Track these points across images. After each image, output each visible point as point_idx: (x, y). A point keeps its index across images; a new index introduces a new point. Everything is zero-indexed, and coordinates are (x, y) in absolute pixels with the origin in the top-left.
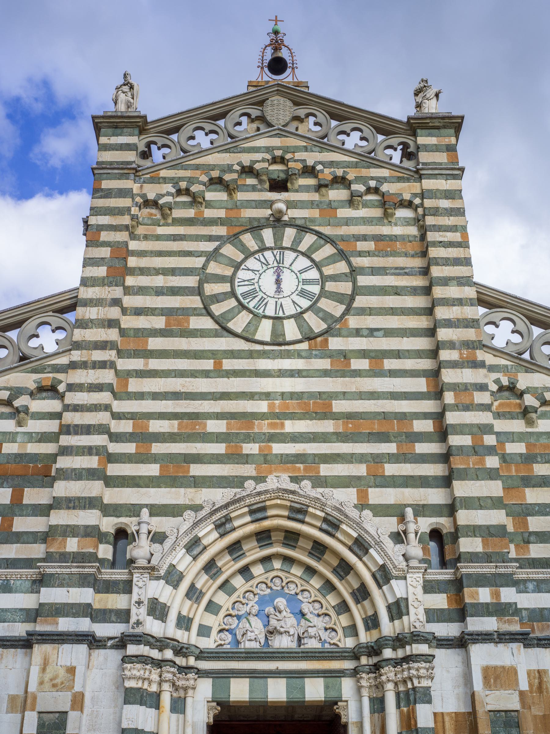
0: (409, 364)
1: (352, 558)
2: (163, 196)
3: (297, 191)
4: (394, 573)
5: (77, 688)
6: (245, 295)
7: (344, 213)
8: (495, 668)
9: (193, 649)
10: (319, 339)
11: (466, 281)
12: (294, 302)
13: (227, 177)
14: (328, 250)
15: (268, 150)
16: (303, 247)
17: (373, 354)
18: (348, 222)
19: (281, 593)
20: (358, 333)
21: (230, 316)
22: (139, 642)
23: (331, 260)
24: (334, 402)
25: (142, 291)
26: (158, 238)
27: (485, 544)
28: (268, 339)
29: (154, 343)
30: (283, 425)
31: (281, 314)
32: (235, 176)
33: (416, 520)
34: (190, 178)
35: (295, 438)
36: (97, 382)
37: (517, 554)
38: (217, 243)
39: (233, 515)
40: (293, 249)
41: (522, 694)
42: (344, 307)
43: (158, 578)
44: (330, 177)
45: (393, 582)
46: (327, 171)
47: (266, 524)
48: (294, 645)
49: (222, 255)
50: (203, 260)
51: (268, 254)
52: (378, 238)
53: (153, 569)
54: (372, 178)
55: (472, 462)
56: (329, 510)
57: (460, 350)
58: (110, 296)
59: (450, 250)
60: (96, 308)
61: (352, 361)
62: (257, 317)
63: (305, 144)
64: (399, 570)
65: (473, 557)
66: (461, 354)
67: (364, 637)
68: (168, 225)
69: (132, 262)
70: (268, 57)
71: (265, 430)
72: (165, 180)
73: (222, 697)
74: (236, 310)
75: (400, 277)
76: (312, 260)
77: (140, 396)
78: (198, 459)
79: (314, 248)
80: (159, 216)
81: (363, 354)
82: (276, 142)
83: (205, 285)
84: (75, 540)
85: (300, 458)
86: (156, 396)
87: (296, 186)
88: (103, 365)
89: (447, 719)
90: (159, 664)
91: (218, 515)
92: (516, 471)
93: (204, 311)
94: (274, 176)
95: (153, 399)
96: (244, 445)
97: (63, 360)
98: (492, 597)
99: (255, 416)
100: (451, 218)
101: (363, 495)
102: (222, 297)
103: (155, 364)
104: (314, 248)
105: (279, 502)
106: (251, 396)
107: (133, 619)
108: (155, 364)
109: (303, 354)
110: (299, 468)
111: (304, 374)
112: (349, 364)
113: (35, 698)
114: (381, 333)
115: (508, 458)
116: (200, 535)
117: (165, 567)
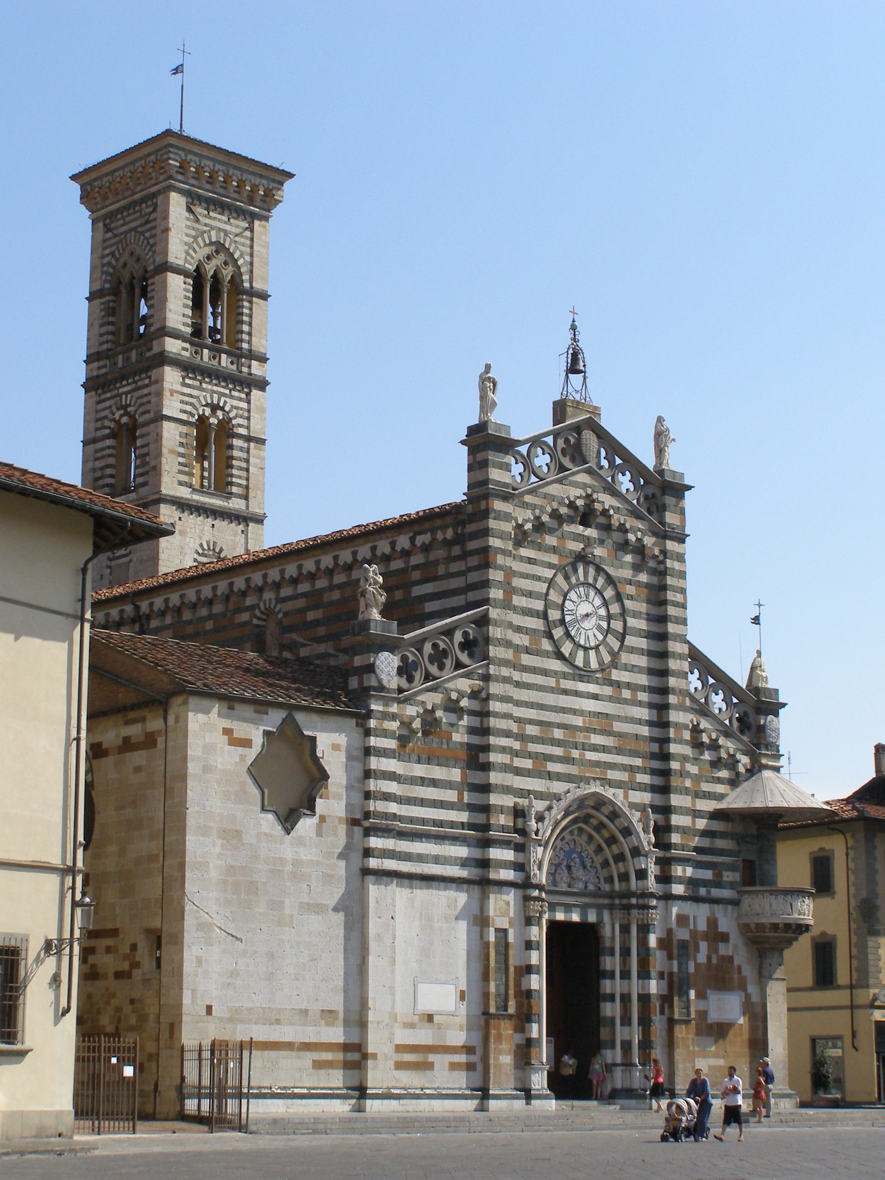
1: (621, 839)
4: (643, 853)
11: (683, 639)
12: (595, 636)
15: (585, 486)
20: (626, 668)
26: (522, 559)
28: (581, 665)
30: (590, 737)
31: (588, 645)
35: (595, 748)
43: (540, 845)
44: (617, 524)
45: (641, 858)
46: (616, 516)
47: (585, 811)
53: (541, 840)
56: (616, 808)
65: (676, 846)
66: (679, 699)
73: (552, 918)
81: (628, 685)
85: (598, 764)
88: (506, 680)
99: (575, 728)
101: (626, 796)
103: (527, 678)
106: (574, 712)
108: (527, 678)
109: (599, 680)
110: (597, 772)
112: (621, 694)
113: (493, 920)
114: (635, 669)
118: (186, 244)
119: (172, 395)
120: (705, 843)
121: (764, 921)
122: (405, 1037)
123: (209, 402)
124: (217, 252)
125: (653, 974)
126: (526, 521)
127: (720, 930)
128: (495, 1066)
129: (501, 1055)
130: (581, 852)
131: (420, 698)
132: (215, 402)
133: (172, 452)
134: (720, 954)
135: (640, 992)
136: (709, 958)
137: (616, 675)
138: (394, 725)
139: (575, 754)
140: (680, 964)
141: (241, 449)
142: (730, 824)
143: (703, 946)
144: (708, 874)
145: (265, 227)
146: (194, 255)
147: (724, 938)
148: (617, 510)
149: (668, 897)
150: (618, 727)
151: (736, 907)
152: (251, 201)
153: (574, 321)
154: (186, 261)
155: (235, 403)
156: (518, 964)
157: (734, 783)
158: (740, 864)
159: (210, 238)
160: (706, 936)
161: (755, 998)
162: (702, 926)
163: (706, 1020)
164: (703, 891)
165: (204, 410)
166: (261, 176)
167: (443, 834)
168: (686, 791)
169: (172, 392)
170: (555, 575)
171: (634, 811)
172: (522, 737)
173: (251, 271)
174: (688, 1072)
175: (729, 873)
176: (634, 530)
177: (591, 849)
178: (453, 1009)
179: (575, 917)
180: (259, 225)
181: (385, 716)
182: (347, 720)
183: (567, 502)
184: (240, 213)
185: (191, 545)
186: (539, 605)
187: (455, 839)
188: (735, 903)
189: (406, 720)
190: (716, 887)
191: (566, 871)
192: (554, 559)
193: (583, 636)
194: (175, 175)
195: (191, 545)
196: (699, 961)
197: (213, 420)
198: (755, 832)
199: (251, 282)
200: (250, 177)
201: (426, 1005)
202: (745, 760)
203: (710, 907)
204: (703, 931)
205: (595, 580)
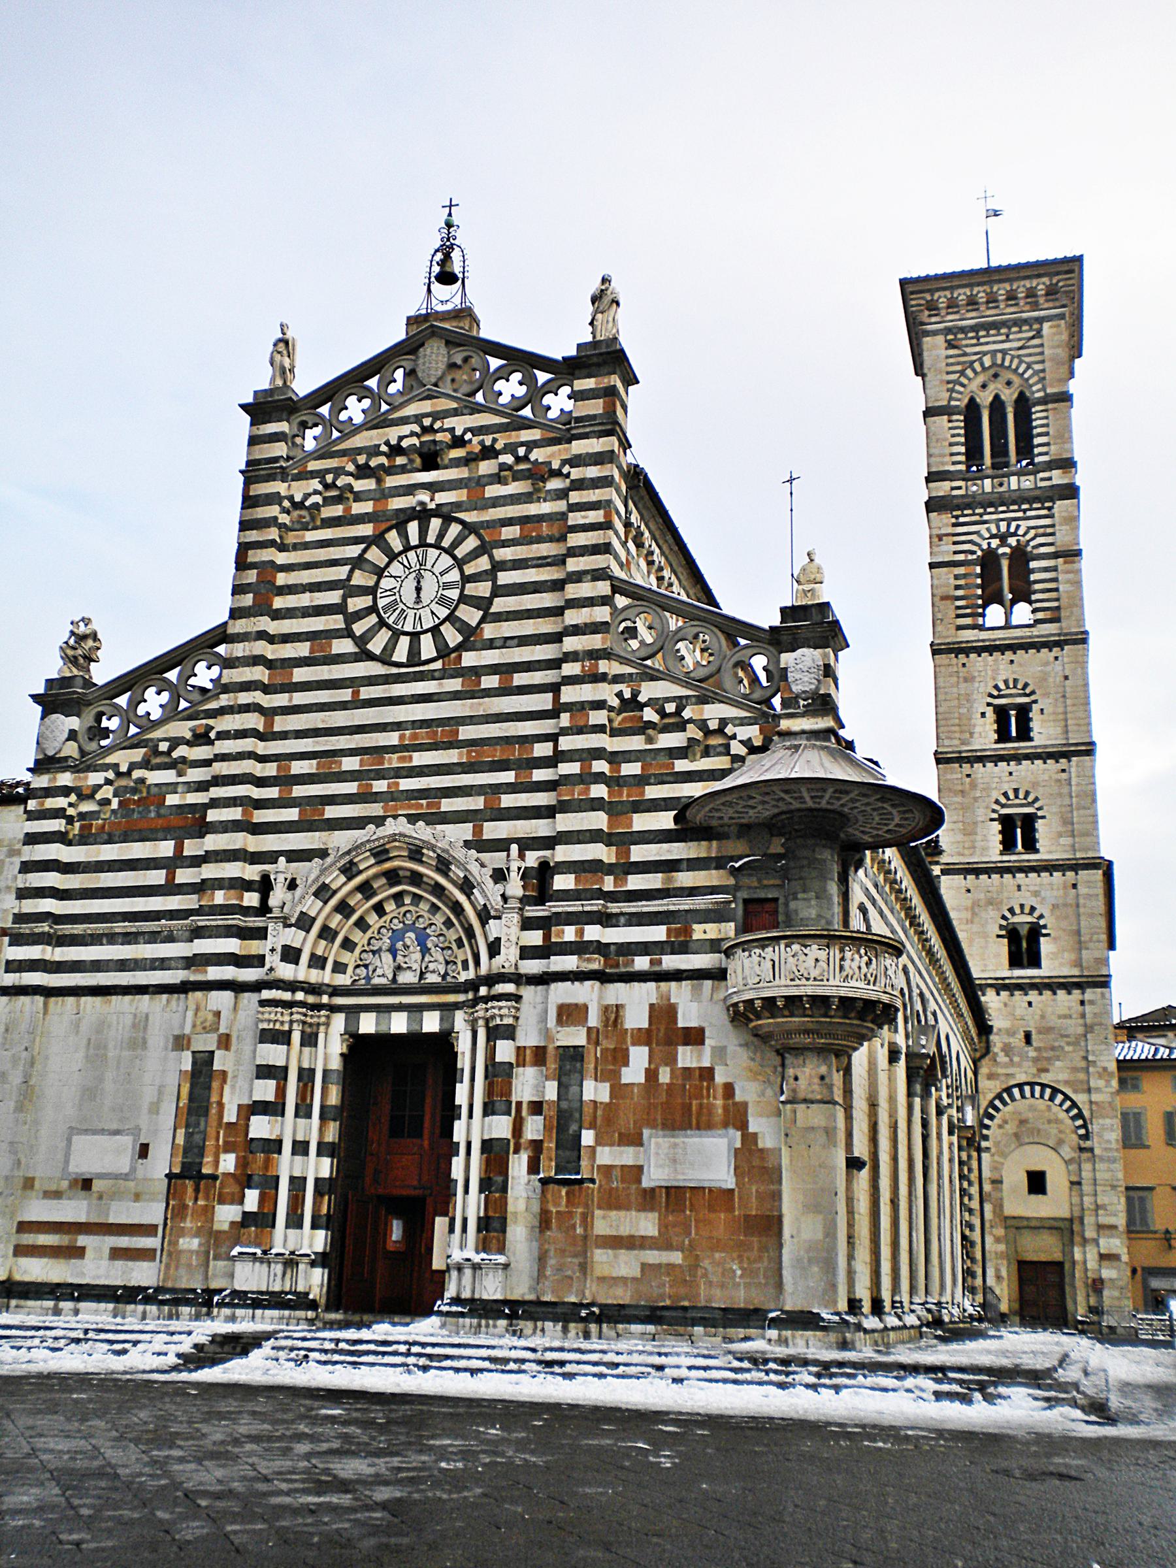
0: (538, 678)
1: (462, 898)
2: (310, 495)
3: (446, 467)
4: (493, 913)
5: (222, 1030)
6: (385, 608)
7: (492, 491)
8: (569, 1005)
9: (324, 988)
10: (453, 655)
12: (432, 613)
13: (373, 463)
14: (472, 543)
15: (418, 419)
16: (446, 543)
17: (504, 669)
18: (496, 502)
19: (412, 928)
20: (491, 644)
21: (370, 634)
22: (271, 988)
23: (474, 555)
24: (461, 728)
25: (289, 613)
26: (306, 546)
27: (577, 880)
29: (300, 674)
30: (411, 758)
31: (419, 629)
32: (383, 460)
33: (522, 856)
34: (336, 468)
36: (241, 728)
37: (615, 886)
38: (363, 546)
39: (356, 860)
40: (436, 546)
41: (589, 1029)
42: (481, 613)
43: (290, 926)
44: (477, 449)
45: (491, 921)
46: (475, 440)
47: (388, 865)
48: (416, 980)
49: (366, 560)
50: (348, 568)
51: (411, 555)
52: (523, 521)
53: (285, 918)
54: (522, 444)
55: (577, 793)
56: (439, 851)
57: (583, 661)
58: (256, 629)
59: (590, 533)
60: (241, 645)
61: (483, 678)
62: (397, 634)
63: (455, 405)
64: (496, 910)
65: (565, 895)
66: (583, 666)
67: (470, 974)
68: (315, 528)
69: (281, 579)
70: (436, 269)
71: (395, 765)
72: (313, 475)
73: (352, 1029)
74: (377, 628)
75: (541, 569)
76: (454, 557)
77: (284, 735)
78: (332, 800)
79: (457, 543)
80: (308, 519)
81: (494, 669)
82: (426, 406)
83: (349, 600)
84: (222, 892)
86: (300, 734)
87: (446, 461)
89: (528, 1052)
90: (289, 1005)
91: (343, 862)
92: (628, 795)
93: (345, 633)
94: (425, 450)
95: (296, 738)
96: (374, 782)
97: (213, 705)
98: (576, 935)
100: (597, 491)
101: (478, 830)
102: (364, 613)
103: (300, 698)
104: (457, 543)
105: (397, 844)
107: (267, 966)
108: (300, 698)
111: (435, 698)
112: (479, 683)
114: (516, 641)
115: (621, 781)
116: (327, 882)
117: (296, 915)
118: (948, 382)
119: (940, 540)
120: (653, 881)
121: (735, 999)
122: (39, 1210)
123: (994, 531)
124: (996, 376)
125: (500, 1106)
126: (307, 496)
127: (680, 1025)
128: (170, 1254)
129: (183, 1236)
130: (425, 929)
131: (110, 759)
132: (1003, 528)
133: (944, 598)
134: (680, 1065)
135: (486, 1137)
136: (651, 1074)
137: (469, 659)
138: (60, 802)
139: (380, 786)
140: (562, 1088)
141: (1046, 570)
142: (714, 843)
143: (639, 1057)
144: (658, 933)
145: (1059, 326)
146: (962, 389)
147: (695, 1037)
148: (475, 431)
149: (544, 979)
150: (467, 733)
151: (724, 983)
152: (1035, 306)
153: (450, 215)
154: (951, 399)
155: (1032, 523)
156: (246, 1101)
157: (723, 774)
158: (737, 907)
159: (982, 364)
160: (644, 1037)
161: (767, 1142)
162: (636, 1018)
163: (639, 1181)
164: (642, 963)
165: (989, 544)
166: (1039, 276)
167: (134, 930)
168: (596, 805)
169: (940, 538)
170: (365, 551)
171: (473, 852)
172: (286, 780)
174: (569, 1273)
175: (708, 926)
176: (511, 448)
177: (439, 919)
178: (126, 1170)
179: (399, 1024)
180: (1051, 327)
181: (48, 792)
182: (13, 808)
183: (384, 448)
184: (1019, 323)
185: (981, 690)
186: (334, 597)
187: (153, 937)
188: (719, 975)
189: (86, 792)
190: (672, 953)
191: (387, 958)
192: (367, 530)
193: (410, 620)
194: (927, 320)
195: (981, 690)
196: (624, 1081)
198: (782, 851)
199: (1044, 389)
200: (1022, 283)
201: (82, 1165)
202: (752, 732)
203: (658, 987)
204: (640, 1029)
205: (441, 536)
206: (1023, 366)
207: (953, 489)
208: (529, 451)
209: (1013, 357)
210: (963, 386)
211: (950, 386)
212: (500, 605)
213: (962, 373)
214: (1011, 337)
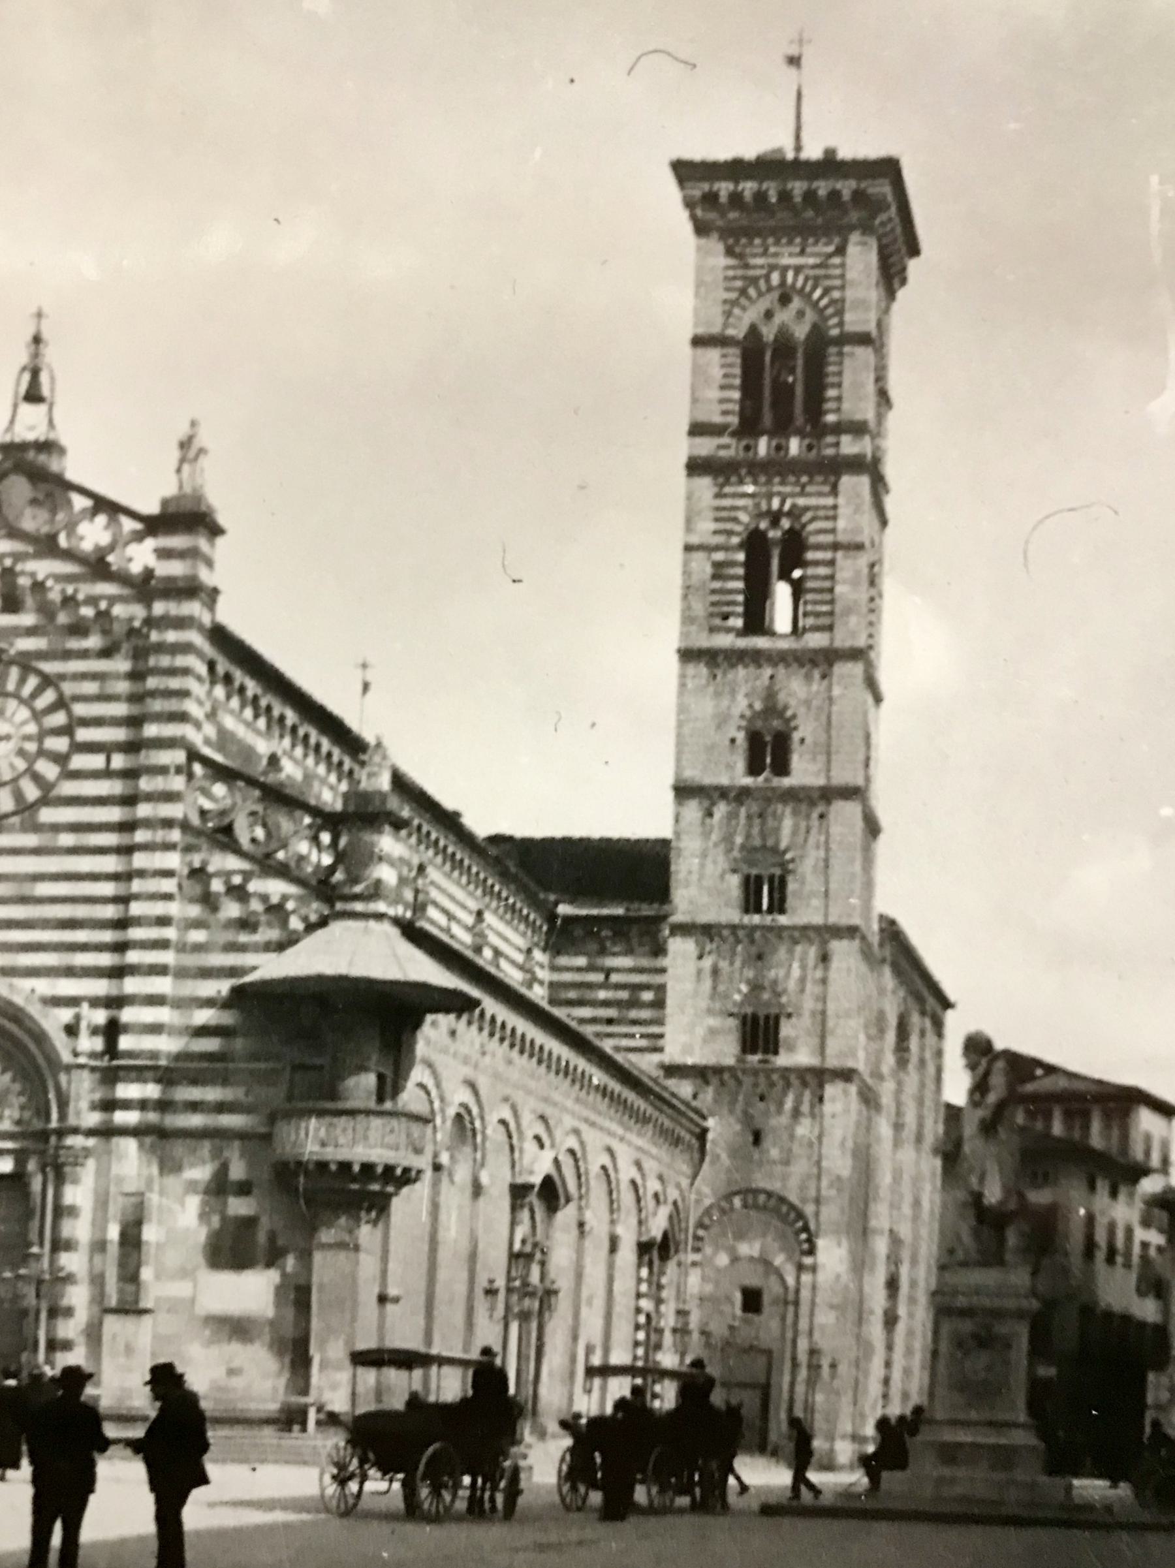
14: (49, 697)
40: (16, 695)
46: (58, 587)
137: (47, 815)
148: (59, 578)
173: (840, 313)
176: (92, 601)
197: (775, 534)
199: (841, 324)
206: (817, 293)
207: (720, 447)
208: (111, 605)
209: (807, 279)
210: (744, 309)
211: (727, 307)
212: (80, 762)
213: (743, 292)
214: (809, 250)
